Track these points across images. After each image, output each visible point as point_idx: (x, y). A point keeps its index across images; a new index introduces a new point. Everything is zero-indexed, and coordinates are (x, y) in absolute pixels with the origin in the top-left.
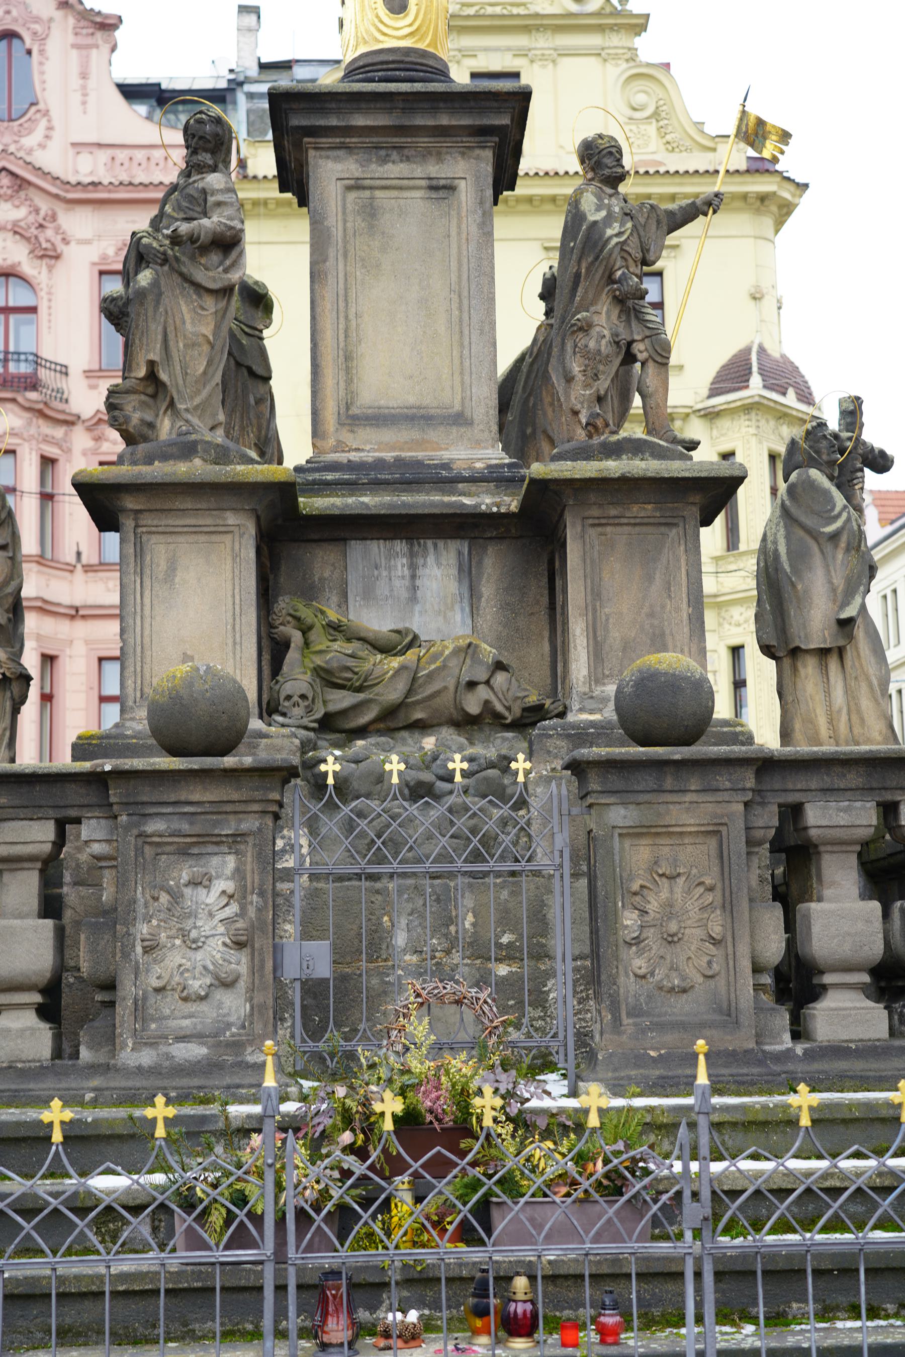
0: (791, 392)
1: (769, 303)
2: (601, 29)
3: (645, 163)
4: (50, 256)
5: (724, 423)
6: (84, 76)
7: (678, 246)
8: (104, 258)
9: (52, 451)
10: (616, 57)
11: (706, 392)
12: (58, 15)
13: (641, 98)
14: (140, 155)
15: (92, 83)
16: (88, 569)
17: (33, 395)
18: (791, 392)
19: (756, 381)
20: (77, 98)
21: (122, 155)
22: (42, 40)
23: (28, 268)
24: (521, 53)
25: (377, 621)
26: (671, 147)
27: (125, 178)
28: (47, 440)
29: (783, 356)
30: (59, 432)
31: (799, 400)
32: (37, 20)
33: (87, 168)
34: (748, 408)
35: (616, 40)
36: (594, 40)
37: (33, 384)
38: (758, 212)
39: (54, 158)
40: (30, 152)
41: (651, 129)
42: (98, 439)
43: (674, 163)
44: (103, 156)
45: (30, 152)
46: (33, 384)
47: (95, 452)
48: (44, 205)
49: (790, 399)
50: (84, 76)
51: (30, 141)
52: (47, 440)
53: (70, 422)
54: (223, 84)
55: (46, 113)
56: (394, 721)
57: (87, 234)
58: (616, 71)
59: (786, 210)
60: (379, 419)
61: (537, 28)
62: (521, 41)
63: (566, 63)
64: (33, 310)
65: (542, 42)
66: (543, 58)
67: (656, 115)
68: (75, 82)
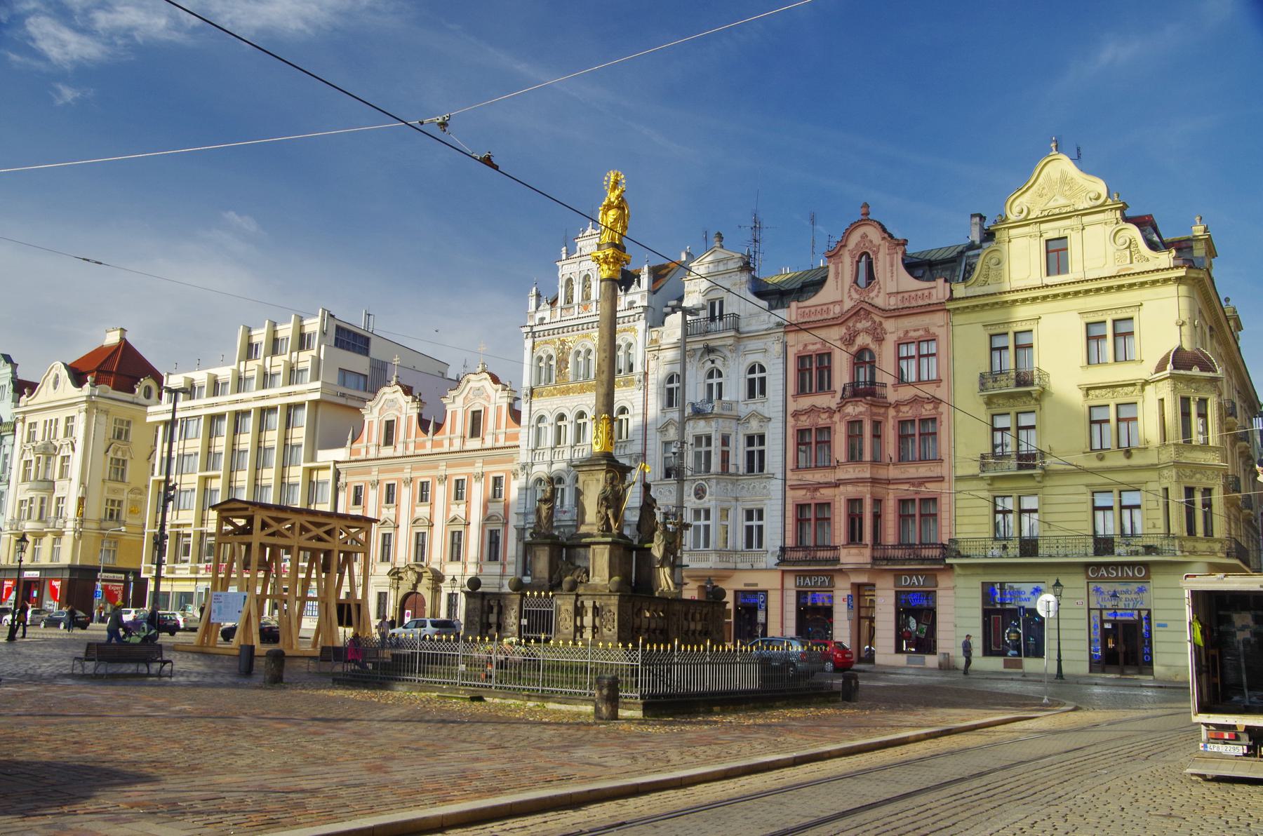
4: (880, 340)
6: (892, 266)
14: (913, 294)
21: (906, 295)
23: (873, 346)
27: (907, 305)
30: (882, 410)
33: (893, 302)
37: (873, 394)
39: (879, 302)
42: (898, 412)
44: (900, 296)
49: (1196, 371)
50: (892, 266)
51: (872, 295)
68: (888, 269)
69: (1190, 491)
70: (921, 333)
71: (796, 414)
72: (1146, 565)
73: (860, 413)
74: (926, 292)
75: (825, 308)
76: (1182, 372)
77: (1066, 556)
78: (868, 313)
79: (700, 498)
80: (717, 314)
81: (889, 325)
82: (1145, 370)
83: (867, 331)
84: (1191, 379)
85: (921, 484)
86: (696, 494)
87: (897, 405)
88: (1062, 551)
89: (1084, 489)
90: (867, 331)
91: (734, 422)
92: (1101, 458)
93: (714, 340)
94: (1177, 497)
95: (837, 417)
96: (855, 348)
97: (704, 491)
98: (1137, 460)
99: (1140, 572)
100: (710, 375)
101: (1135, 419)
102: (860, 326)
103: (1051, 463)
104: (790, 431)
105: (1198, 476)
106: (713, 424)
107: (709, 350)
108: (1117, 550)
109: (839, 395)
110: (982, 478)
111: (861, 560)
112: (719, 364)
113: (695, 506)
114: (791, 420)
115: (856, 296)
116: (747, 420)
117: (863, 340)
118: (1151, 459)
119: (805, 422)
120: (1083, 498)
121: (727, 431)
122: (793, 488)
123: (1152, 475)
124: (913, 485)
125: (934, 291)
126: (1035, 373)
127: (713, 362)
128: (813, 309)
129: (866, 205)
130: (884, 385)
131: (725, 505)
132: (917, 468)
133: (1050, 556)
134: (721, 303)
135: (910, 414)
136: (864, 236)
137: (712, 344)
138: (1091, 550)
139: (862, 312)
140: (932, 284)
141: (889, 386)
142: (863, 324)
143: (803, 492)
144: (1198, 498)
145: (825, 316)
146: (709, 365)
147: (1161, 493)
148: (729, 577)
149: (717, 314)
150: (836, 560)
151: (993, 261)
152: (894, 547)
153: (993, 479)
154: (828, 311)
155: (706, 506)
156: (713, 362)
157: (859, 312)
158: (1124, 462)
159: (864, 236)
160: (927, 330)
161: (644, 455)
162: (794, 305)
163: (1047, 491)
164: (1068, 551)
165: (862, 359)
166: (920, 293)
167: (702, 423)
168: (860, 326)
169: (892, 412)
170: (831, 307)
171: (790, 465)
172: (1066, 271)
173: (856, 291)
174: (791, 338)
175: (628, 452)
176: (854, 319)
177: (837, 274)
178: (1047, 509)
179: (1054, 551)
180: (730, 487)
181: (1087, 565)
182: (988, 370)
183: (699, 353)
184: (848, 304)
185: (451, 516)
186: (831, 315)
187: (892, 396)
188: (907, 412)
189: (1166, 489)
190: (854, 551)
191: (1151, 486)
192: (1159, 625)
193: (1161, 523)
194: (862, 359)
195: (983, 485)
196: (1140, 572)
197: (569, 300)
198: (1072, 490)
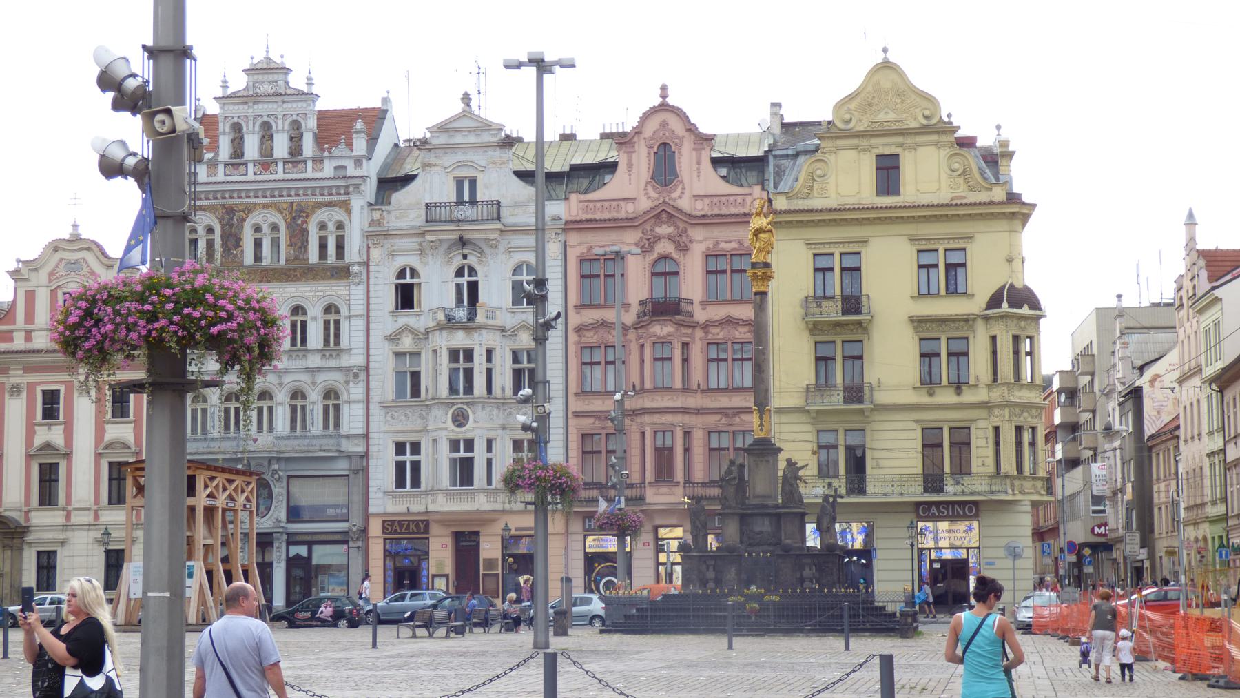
0: (1026, 306)
1: (1017, 263)
2: (938, 133)
3: (957, 198)
4: (684, 249)
5: (993, 322)
6: (698, 163)
8: (708, 249)
9: (687, 340)
10: (944, 146)
11: (984, 306)
12: (686, 134)
13: (956, 166)
14: (723, 199)
15: (702, 167)
16: (703, 391)
17: (678, 317)
18: (1026, 306)
19: (1005, 305)
20: (695, 174)
21: (716, 200)
22: (679, 146)
23: (675, 255)
25: (757, 529)
27: (716, 211)
28: (685, 335)
29: (1026, 287)
30: (689, 331)
31: (1030, 308)
32: (677, 137)
33: (701, 208)
34: (1002, 317)
36: (934, 138)
38: (1011, 219)
39: (685, 204)
40: (675, 200)
41: (961, 180)
42: (706, 333)
44: (707, 201)
45: (675, 200)
46: (678, 312)
47: (705, 338)
48: (681, 225)
50: (698, 163)
51: (674, 195)
52: (685, 335)
53: (694, 326)
54: (761, 153)
55: (682, 182)
56: (758, 544)
57: (701, 239)
58: (944, 153)
59: (1025, 218)
60: (758, 497)
62: (900, 140)
63: (922, 150)
64: (677, 273)
65: (909, 140)
66: (909, 148)
67: (964, 173)
68: (695, 167)
69: (1019, 429)
70: (734, 245)
71: (579, 330)
73: (669, 334)
74: (740, 199)
75: (614, 204)
76: (1015, 310)
78: (671, 216)
79: (460, 426)
80: (466, 198)
81: (697, 234)
82: (975, 305)
83: (670, 238)
84: (1021, 317)
85: (734, 415)
86: (455, 420)
87: (706, 326)
88: (897, 490)
89: (914, 425)
90: (670, 238)
91: (498, 333)
93: (472, 232)
94: (1008, 436)
95: (632, 335)
96: (655, 256)
97: (466, 418)
98: (968, 397)
99: (970, 510)
100: (460, 273)
101: (966, 354)
102: (659, 230)
103: (882, 397)
104: (572, 348)
105: (1026, 414)
106: (476, 335)
107: (462, 242)
109: (635, 309)
110: (808, 412)
111: (672, 499)
112: (472, 260)
113: (453, 436)
114: (573, 337)
115: (653, 194)
116: (514, 333)
117: (664, 247)
118: (981, 395)
119: (591, 338)
120: (912, 434)
121: (491, 345)
122: (578, 415)
123: (983, 413)
124: (726, 415)
125: (749, 199)
126: (864, 300)
127: (465, 257)
128: (599, 205)
129: (664, 88)
130: (691, 302)
131: (492, 434)
132: (730, 397)
134: (473, 182)
135: (721, 335)
136: (664, 124)
137: (467, 236)
138: (921, 489)
139: (664, 215)
140: (746, 190)
141: (696, 302)
142: (664, 230)
143: (591, 420)
144: (1026, 437)
145: (614, 215)
146: (458, 261)
147: (991, 434)
148: (494, 520)
149: (466, 198)
150: (642, 499)
151: (819, 172)
152: (704, 485)
153: (818, 412)
154: (618, 209)
155: (469, 435)
156: (465, 257)
157: (664, 214)
159: (664, 124)
160: (740, 243)
161: (367, 368)
162: (574, 197)
163: (876, 426)
164: (904, 490)
165: (664, 270)
166: (731, 198)
167: (460, 334)
168: (659, 230)
169: (699, 333)
170: (622, 204)
171: (573, 388)
172: (898, 193)
173: (655, 189)
174: (573, 238)
175: (344, 363)
176: (653, 221)
177: (630, 166)
180: (495, 412)
182: (812, 294)
183: (445, 246)
184: (644, 204)
185: (38, 442)
186: (622, 215)
187: (700, 315)
188: (718, 334)
189: (997, 429)
190: (664, 490)
191: (982, 424)
192: (988, 564)
193: (990, 461)
194: (664, 270)
195: (803, 418)
196: (970, 510)
197: (238, 152)
198: (900, 425)
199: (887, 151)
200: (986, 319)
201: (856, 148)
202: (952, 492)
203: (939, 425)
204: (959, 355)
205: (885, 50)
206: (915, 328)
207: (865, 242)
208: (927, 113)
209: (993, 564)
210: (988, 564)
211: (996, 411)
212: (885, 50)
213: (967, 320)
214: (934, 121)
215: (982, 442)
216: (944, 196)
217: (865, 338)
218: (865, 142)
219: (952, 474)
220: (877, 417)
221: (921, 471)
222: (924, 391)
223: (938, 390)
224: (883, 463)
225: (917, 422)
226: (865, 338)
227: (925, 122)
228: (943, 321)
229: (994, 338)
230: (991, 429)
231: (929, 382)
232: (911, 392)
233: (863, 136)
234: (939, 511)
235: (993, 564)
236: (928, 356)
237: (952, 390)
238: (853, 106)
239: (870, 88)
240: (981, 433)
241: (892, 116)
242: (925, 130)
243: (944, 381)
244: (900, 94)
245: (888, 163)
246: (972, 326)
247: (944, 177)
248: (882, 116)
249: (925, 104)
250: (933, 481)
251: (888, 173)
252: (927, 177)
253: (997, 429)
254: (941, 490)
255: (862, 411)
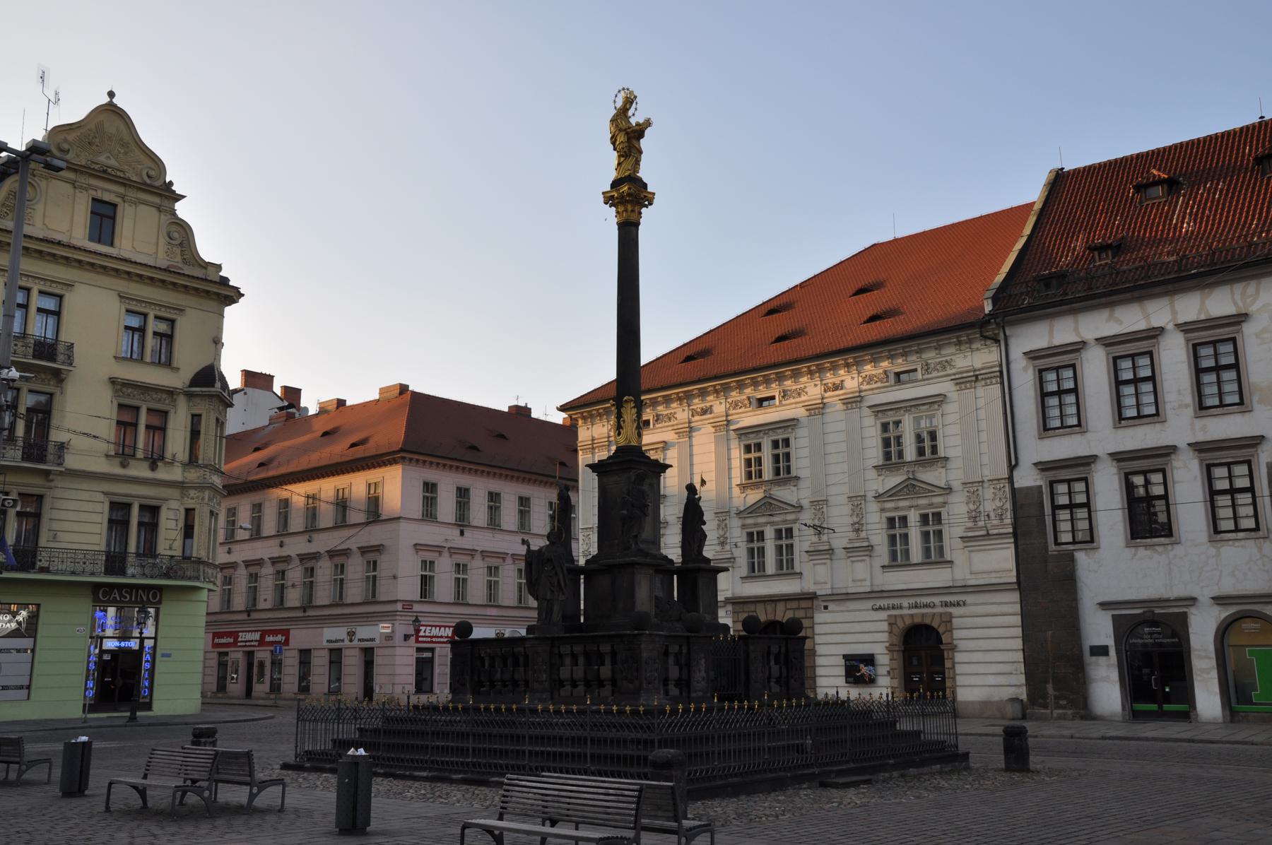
2: (161, 195)
5: (198, 400)
7: (182, 310)
11: (188, 383)
24: (123, 197)
26: (185, 261)
34: (211, 396)
35: (166, 203)
36: (156, 200)
41: (178, 251)
43: (187, 270)
58: (165, 218)
61: (130, 186)
62: (121, 190)
65: (132, 194)
67: (181, 244)
72: (160, 588)
77: (92, 574)
82: (178, 380)
88: (89, 568)
89: (101, 497)
92: (124, 466)
98: (162, 474)
103: (71, 462)
108: (130, 571)
118: (176, 474)
120: (99, 507)
123: (175, 493)
126: (61, 348)
133: (73, 573)
158: (147, 474)
163: (58, 493)
178: (55, 514)
179: (79, 568)
181: (96, 587)
198: (85, 496)
199: (107, 197)
200: (190, 396)
201: (73, 184)
202: (134, 575)
203: (125, 500)
204: (159, 429)
205: (111, 94)
206: (116, 391)
207: (70, 286)
208: (152, 173)
209: (168, 655)
210: (163, 655)
211: (192, 493)
212: (111, 94)
213: (171, 393)
214: (158, 183)
215: (172, 524)
216: (162, 263)
217: (58, 391)
218: (83, 180)
219: (138, 555)
220: (59, 482)
221: (103, 548)
222: (118, 460)
223: (132, 462)
224: (61, 536)
225: (105, 493)
226: (58, 391)
227: (148, 181)
228: (145, 389)
229: (196, 418)
230: (183, 511)
231: (124, 454)
232: (103, 459)
233: (82, 172)
234: (121, 595)
235: (168, 655)
236: (126, 426)
237: (146, 465)
238: (71, 137)
239: (92, 126)
240: (171, 515)
241: (113, 162)
242: (144, 188)
243: (140, 454)
244: (124, 145)
245: (107, 210)
246: (175, 401)
247: (162, 241)
248: (102, 159)
249: (149, 163)
250: (115, 562)
251: (104, 219)
252: (136, 237)
253: (189, 512)
254: (123, 573)
255: (47, 473)
